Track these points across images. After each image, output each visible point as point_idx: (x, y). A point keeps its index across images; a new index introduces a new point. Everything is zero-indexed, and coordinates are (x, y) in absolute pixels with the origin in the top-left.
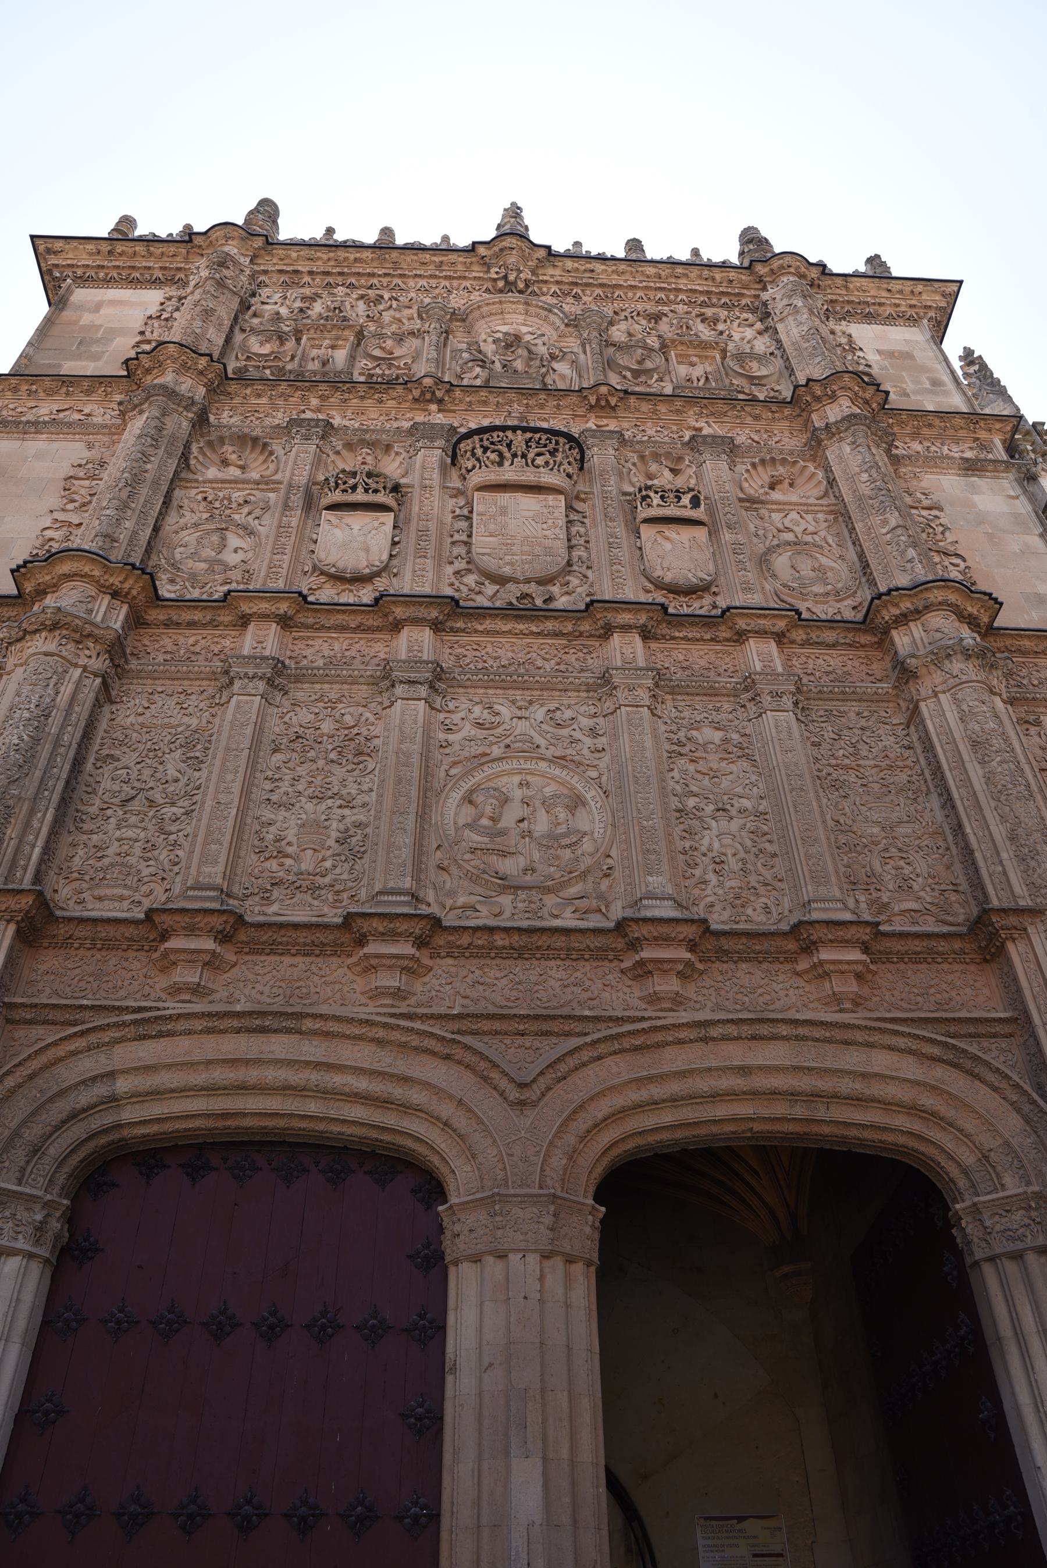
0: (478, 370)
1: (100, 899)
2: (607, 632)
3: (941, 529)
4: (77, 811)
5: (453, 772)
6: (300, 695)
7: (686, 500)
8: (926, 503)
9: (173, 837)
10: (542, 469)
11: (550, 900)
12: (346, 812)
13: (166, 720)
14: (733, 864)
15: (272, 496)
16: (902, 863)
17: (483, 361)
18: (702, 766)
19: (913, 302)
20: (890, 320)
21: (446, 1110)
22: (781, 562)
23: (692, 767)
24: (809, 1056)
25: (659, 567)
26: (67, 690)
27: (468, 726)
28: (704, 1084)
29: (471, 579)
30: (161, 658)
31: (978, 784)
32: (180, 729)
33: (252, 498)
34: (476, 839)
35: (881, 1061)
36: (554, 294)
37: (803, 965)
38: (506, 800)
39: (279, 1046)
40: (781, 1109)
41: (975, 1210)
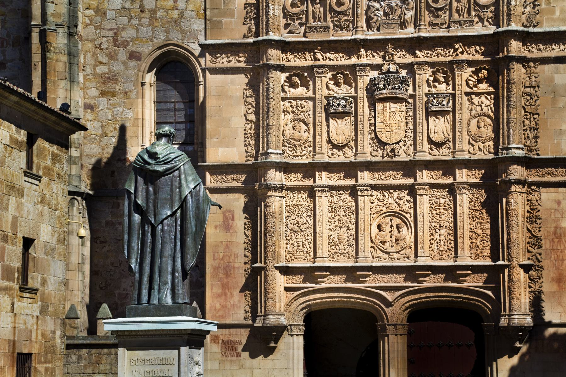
1: (296, 258)
3: (536, 98)
4: (285, 234)
5: (374, 216)
7: (445, 103)
9: (308, 241)
10: (398, 91)
11: (397, 255)
12: (348, 231)
13: (300, 203)
16: (485, 242)
17: (378, 10)
23: (434, 212)
25: (433, 132)
27: (376, 201)
30: (293, 179)
32: (304, 205)
33: (305, 104)
34: (381, 239)
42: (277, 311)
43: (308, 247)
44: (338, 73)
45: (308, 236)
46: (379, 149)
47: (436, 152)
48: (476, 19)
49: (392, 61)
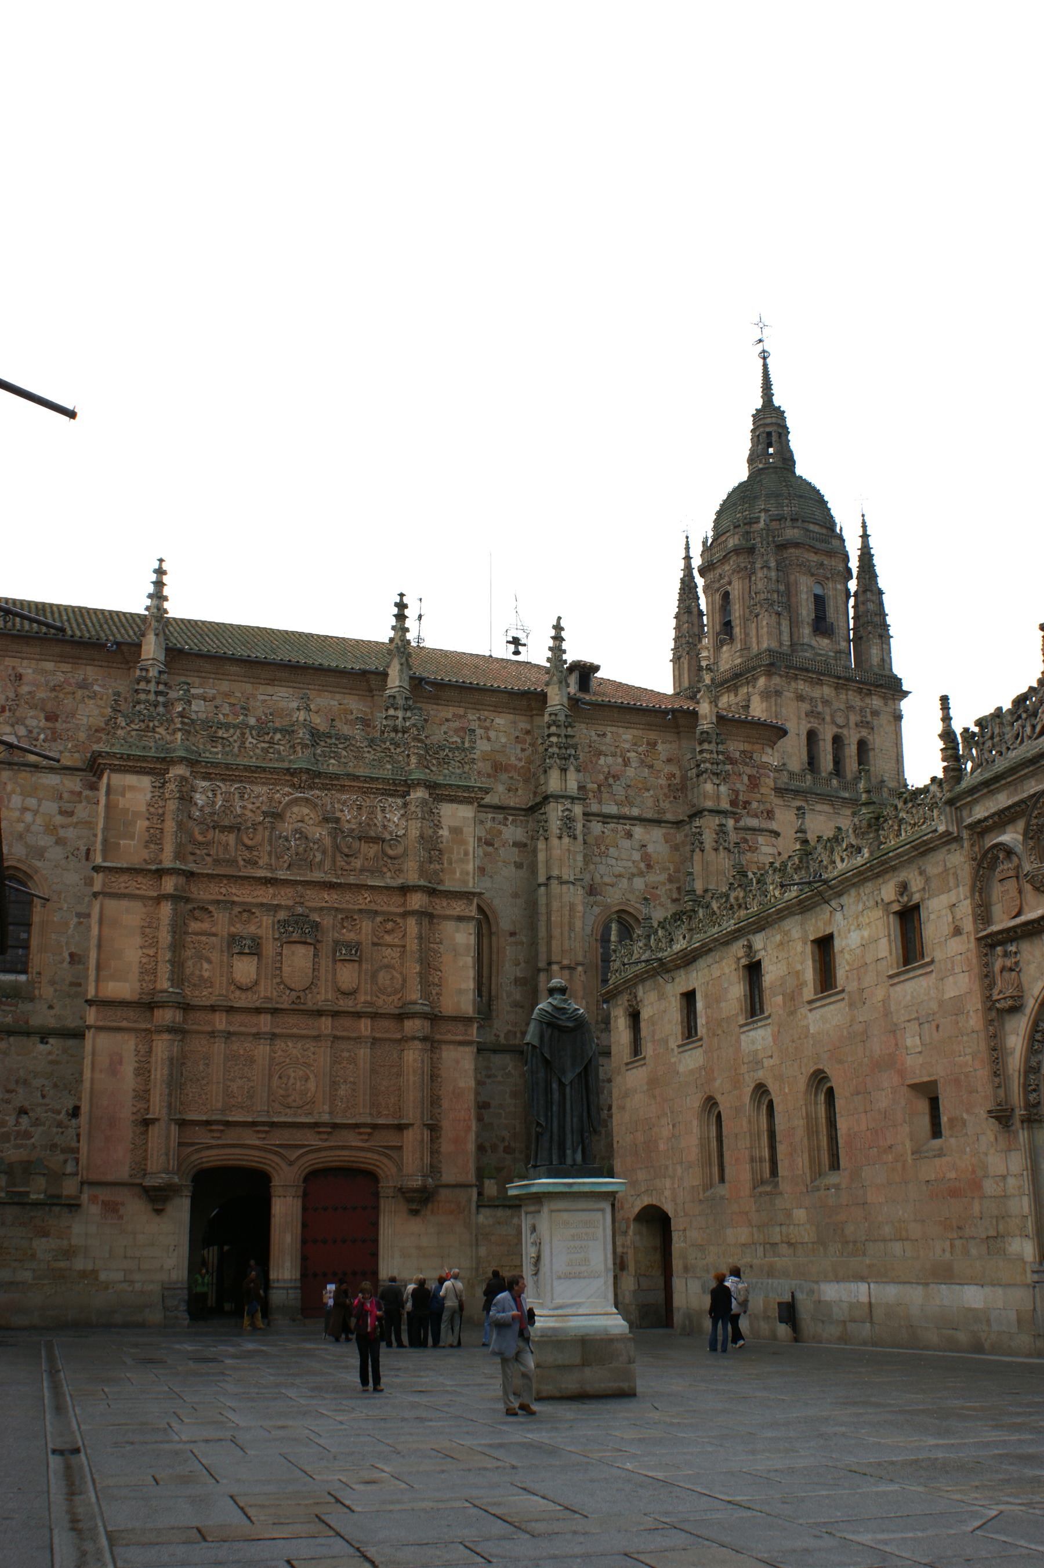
0: (286, 857)
2: (322, 1015)
6: (234, 1039)
7: (353, 952)
8: (438, 940)
11: (299, 1111)
14: (345, 1099)
15: (214, 938)
18: (342, 1066)
19: (473, 795)
20: (460, 802)
21: (273, 1165)
22: (381, 974)
24: (354, 1153)
26: (175, 1049)
28: (331, 1159)
29: (282, 987)
31: (411, 1082)
34: (282, 1092)
35: (369, 1155)
36: (319, 789)
37: (357, 1131)
38: (289, 1078)
39: (237, 1151)
40: (346, 1164)
41: (382, 1187)
42: (171, 1169)
43: (204, 1097)
44: (245, 911)
45: (205, 1085)
46: (284, 996)
47: (341, 1003)
48: (385, 870)
49: (303, 903)
